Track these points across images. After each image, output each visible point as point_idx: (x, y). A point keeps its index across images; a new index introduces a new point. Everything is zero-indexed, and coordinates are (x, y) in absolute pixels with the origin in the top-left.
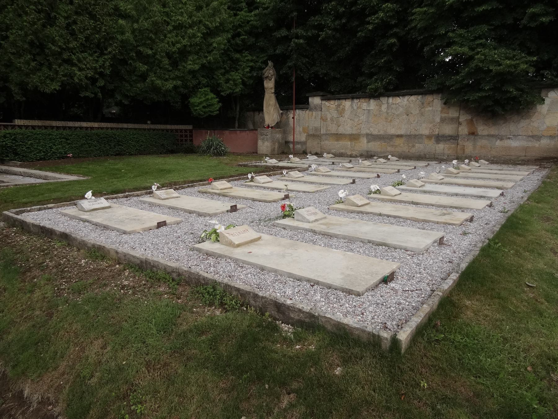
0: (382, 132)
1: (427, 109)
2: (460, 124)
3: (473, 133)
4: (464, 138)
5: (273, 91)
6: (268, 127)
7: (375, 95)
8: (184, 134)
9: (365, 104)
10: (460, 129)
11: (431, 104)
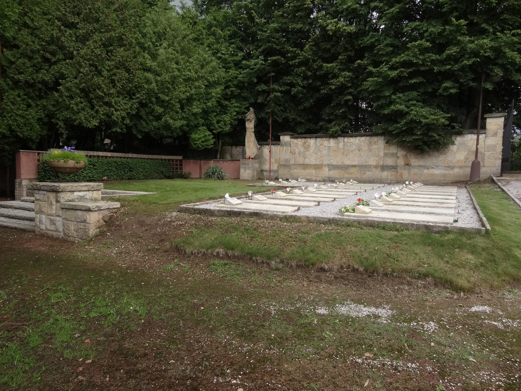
0: (340, 163)
1: (373, 147)
2: (398, 157)
5: (253, 130)
6: (249, 158)
7: (334, 136)
9: (326, 142)
10: (398, 161)
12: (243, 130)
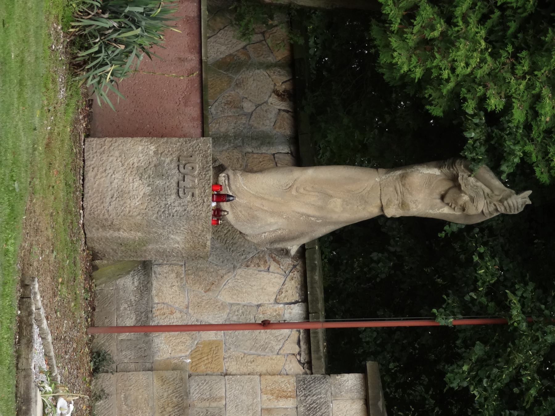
5: (392, 212)
6: (221, 197)
12: (394, 152)
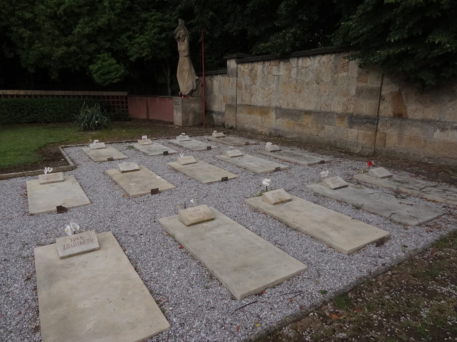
0: (291, 107)
1: (340, 75)
2: (381, 98)
3: (400, 116)
4: (386, 121)
7: (285, 57)
8: (120, 100)
9: (275, 68)
10: (382, 107)
11: (345, 68)
12: (176, 54)
